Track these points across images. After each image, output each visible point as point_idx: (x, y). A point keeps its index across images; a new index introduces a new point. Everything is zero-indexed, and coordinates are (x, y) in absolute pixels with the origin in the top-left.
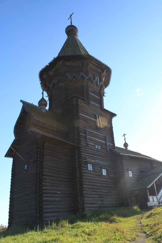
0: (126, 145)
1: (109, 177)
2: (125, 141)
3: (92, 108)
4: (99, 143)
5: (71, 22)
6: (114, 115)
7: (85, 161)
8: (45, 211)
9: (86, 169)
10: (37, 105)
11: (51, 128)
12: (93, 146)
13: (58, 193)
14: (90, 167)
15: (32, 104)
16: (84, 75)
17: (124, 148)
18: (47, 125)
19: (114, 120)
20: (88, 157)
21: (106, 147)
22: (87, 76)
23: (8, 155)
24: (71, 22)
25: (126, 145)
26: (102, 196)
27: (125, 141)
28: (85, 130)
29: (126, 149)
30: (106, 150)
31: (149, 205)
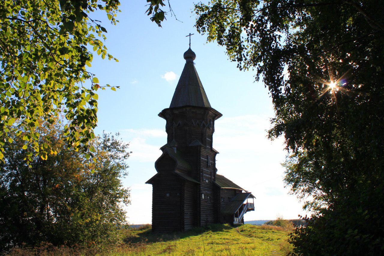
4: (207, 178)
5: (190, 44)
6: (218, 153)
8: (185, 224)
13: (189, 213)
16: (205, 123)
19: (217, 157)
20: (202, 190)
21: (211, 180)
23: (149, 182)
24: (190, 44)
26: (207, 215)
28: (202, 170)
30: (211, 182)
31: (234, 224)
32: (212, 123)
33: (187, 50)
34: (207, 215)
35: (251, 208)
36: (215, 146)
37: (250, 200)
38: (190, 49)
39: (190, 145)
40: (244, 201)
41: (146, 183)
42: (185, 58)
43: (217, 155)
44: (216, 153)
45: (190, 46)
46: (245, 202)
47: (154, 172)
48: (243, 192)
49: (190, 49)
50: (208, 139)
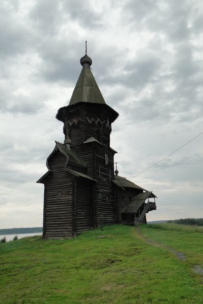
4: (105, 177)
6: (117, 152)
14: (100, 195)
19: (115, 156)
22: (102, 122)
23: (41, 181)
29: (117, 175)
32: (108, 122)
33: (84, 56)
35: (153, 207)
36: (113, 146)
37: (151, 200)
38: (86, 55)
39: (85, 142)
40: (145, 199)
41: (37, 182)
42: (82, 64)
43: (115, 155)
44: (114, 152)
46: (146, 202)
47: (44, 170)
48: (144, 191)
49: (86, 55)
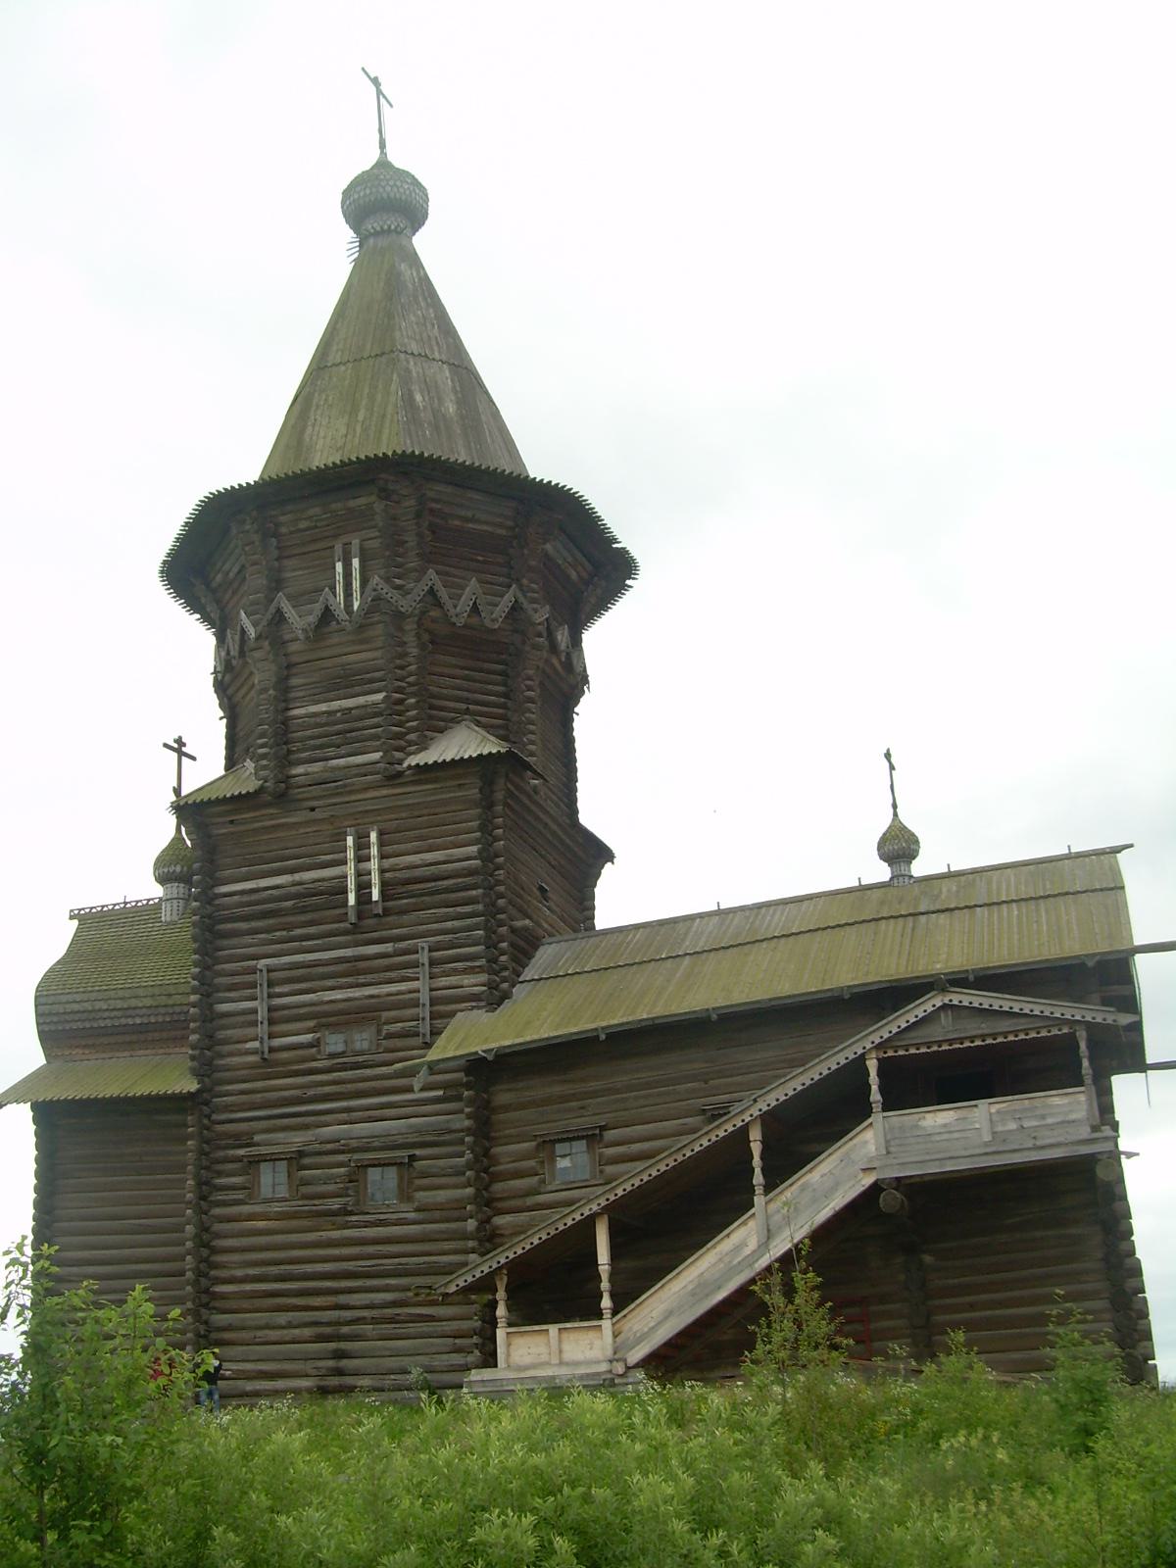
0: (898, 846)
1: (417, 1210)
2: (895, 814)
3: (313, 809)
7: (241, 1152)
9: (240, 1195)
10: (157, 891)
11: (130, 1021)
12: (310, 1045)
14: (272, 1181)
15: (126, 903)
17: (882, 872)
18: (106, 1014)
25: (898, 846)
26: (345, 1330)
27: (895, 814)
28: (254, 971)
34: (345, 1330)
45: (382, 145)
50: (323, 707)
